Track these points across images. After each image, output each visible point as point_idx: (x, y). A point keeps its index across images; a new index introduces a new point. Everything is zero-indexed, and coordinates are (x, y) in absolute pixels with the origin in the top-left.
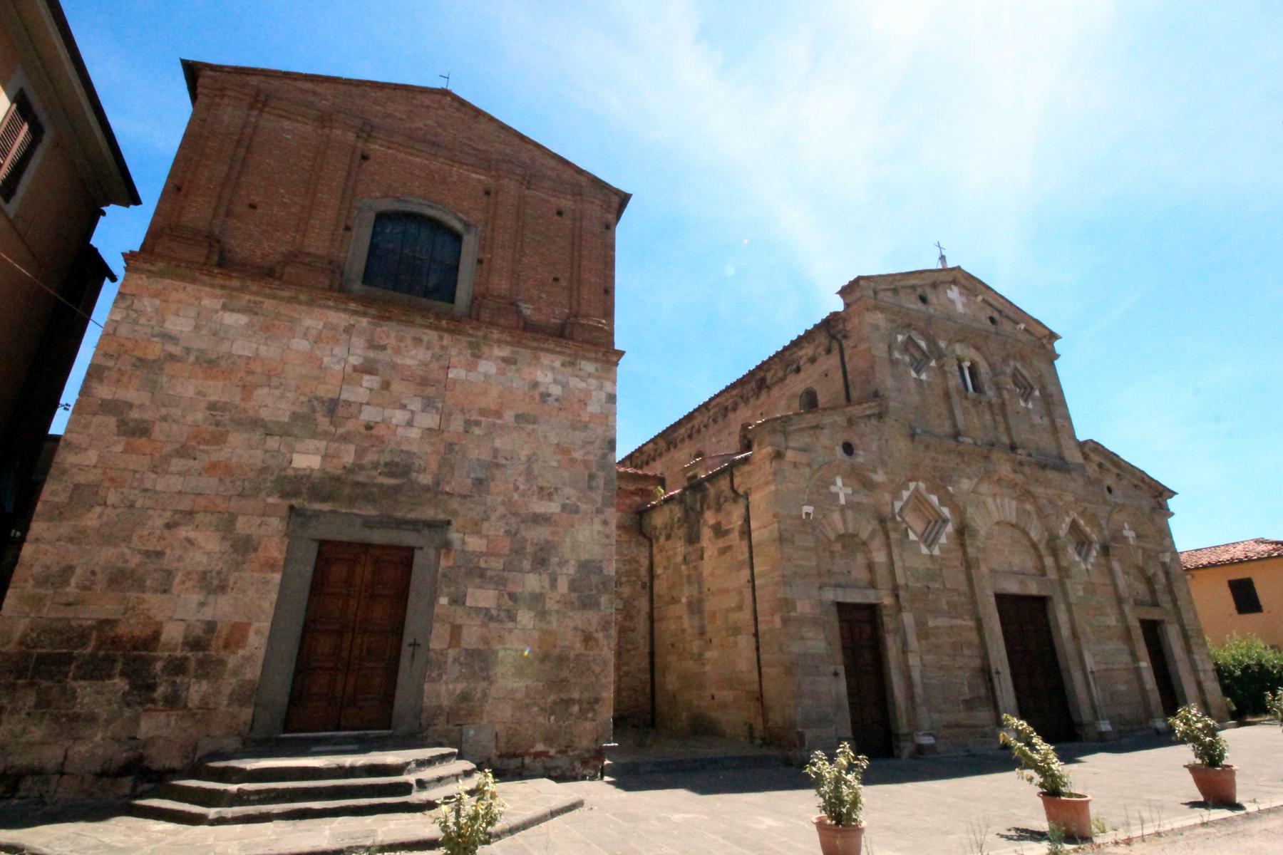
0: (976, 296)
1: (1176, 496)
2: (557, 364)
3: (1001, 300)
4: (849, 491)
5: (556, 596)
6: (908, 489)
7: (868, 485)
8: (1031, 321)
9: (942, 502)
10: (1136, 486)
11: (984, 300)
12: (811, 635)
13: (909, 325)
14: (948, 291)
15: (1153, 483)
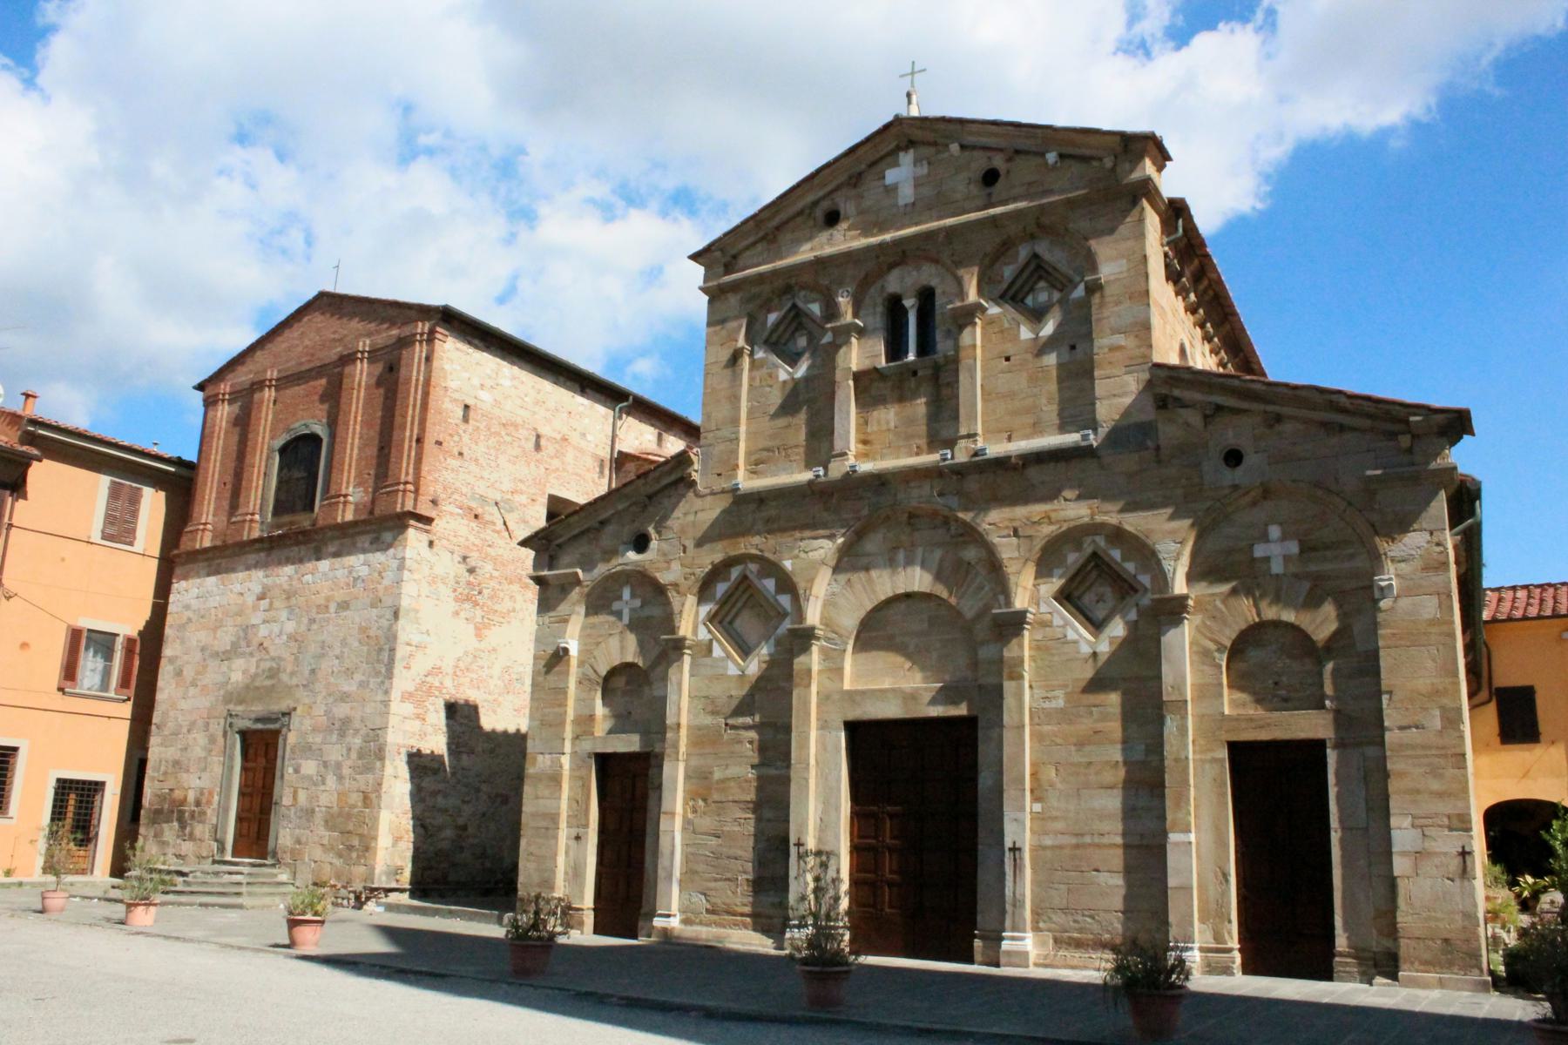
2: (367, 545)
3: (994, 127)
4: (637, 603)
5: (349, 763)
10: (1324, 425)
11: (963, 147)
13: (788, 290)
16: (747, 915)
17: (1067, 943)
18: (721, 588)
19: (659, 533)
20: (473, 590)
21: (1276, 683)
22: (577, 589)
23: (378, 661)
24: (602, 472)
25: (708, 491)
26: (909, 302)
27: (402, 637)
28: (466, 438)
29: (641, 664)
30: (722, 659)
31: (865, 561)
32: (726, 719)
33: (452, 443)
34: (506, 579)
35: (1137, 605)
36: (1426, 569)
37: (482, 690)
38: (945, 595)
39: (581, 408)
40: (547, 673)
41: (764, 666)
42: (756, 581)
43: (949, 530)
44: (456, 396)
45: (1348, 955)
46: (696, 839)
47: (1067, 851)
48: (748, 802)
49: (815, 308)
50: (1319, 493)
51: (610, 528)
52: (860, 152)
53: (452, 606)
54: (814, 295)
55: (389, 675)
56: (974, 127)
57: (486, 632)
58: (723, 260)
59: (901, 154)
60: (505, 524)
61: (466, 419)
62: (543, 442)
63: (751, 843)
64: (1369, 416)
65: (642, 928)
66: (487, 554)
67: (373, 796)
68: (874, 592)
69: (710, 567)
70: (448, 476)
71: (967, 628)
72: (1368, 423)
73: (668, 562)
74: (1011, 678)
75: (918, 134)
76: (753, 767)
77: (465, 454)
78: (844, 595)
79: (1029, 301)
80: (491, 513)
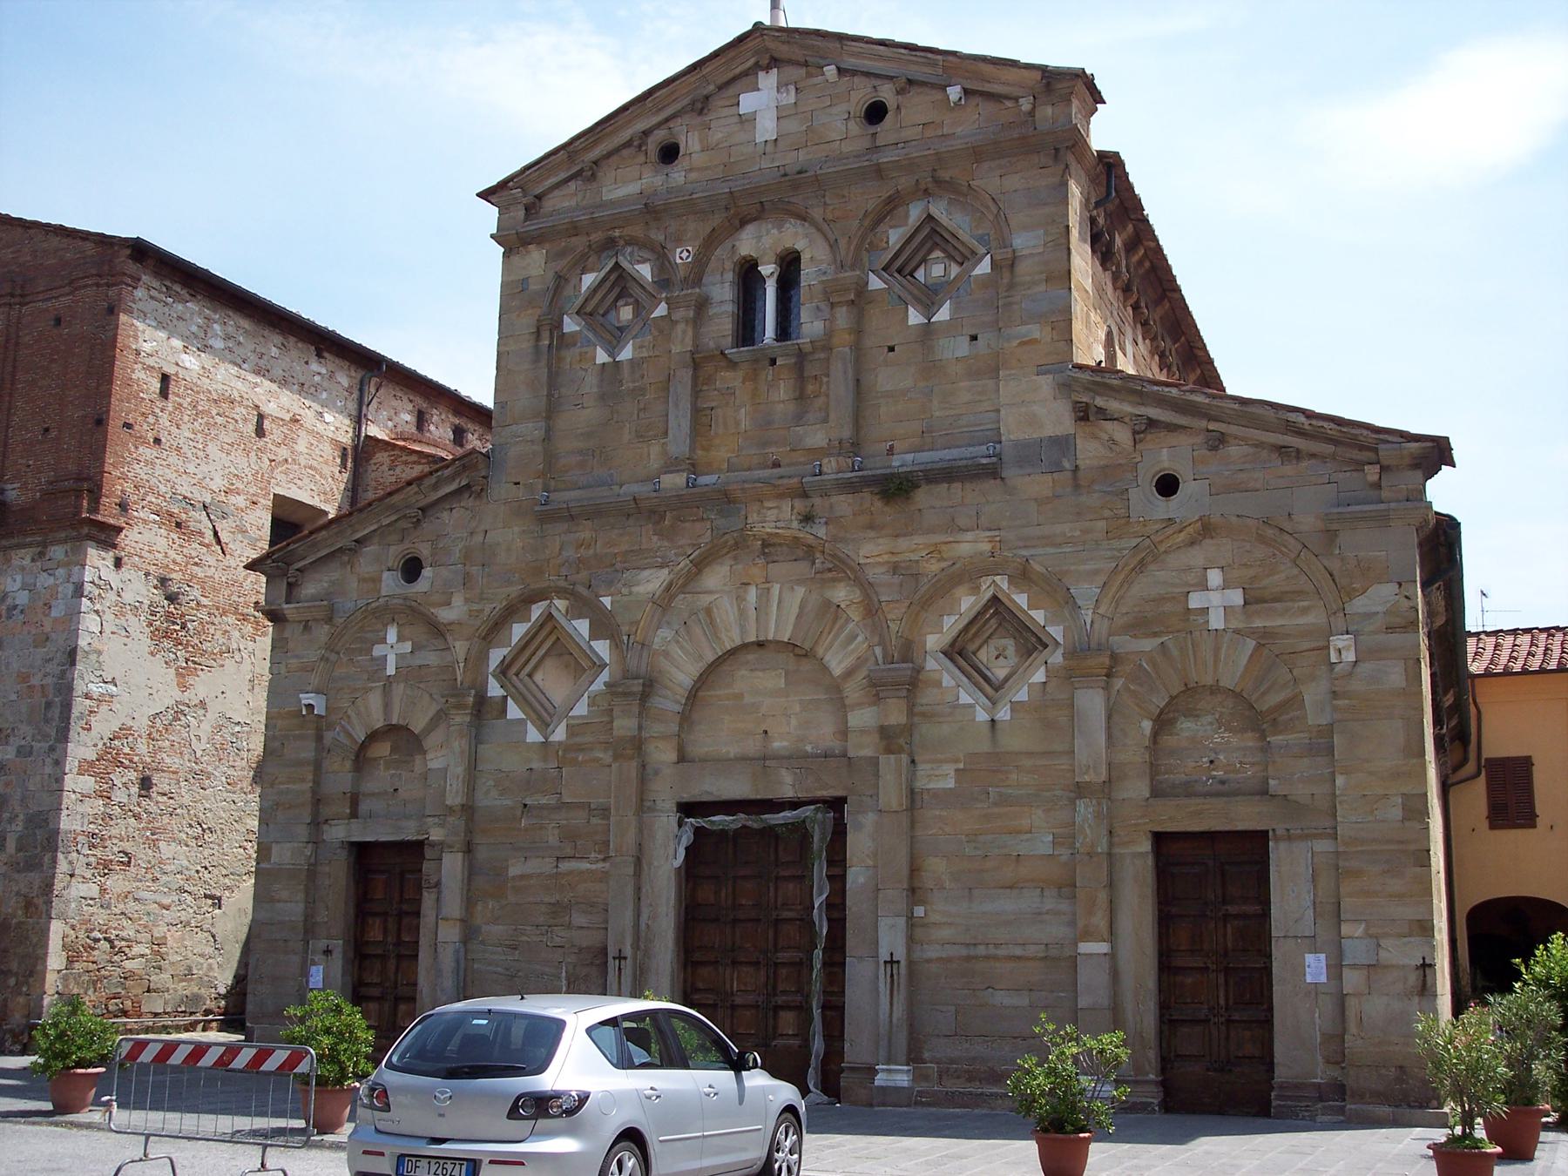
2: (27, 562)
7: (438, 631)
9: (594, 635)
10: (1281, 450)
12: (285, 894)
20: (174, 623)
21: (1212, 762)
23: (47, 721)
24: (344, 465)
26: (767, 269)
27: (79, 687)
28: (164, 420)
33: (145, 427)
34: (218, 610)
36: (1390, 629)
37: (186, 757)
39: (317, 378)
42: (563, 621)
43: (814, 563)
44: (150, 361)
49: (645, 271)
50: (1270, 532)
51: (371, 549)
52: (706, 70)
53: (146, 643)
54: (646, 254)
55: (63, 736)
57: (190, 680)
58: (525, 200)
59: (761, 74)
60: (216, 534)
61: (164, 393)
62: (267, 424)
66: (193, 576)
67: (40, 901)
70: (140, 470)
72: (1330, 448)
75: (783, 50)
77: (163, 440)
78: (678, 642)
79: (920, 275)
80: (199, 520)
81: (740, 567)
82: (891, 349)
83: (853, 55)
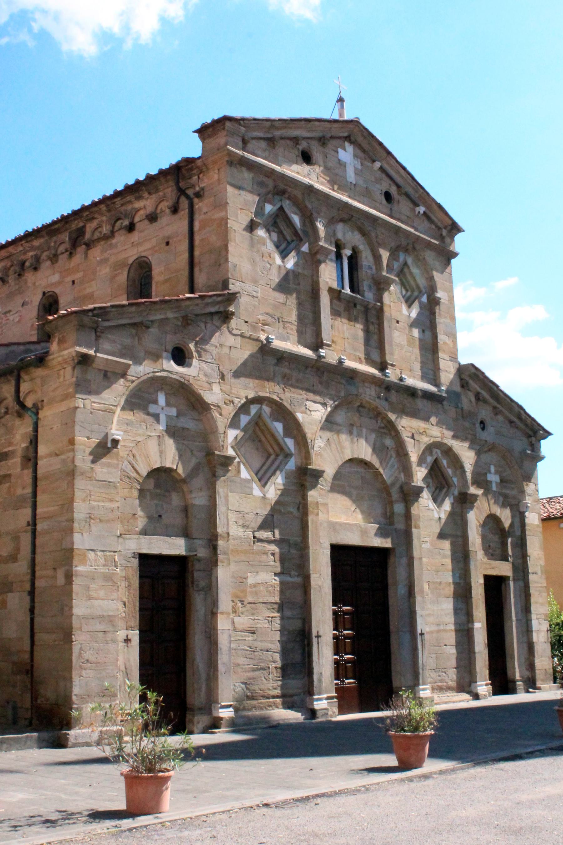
0: (374, 161)
1: (550, 437)
3: (402, 171)
4: (173, 412)
6: (247, 413)
8: (434, 204)
10: (511, 422)
11: (381, 169)
14: (340, 150)
15: (529, 421)
16: (277, 697)
17: (437, 690)
18: (244, 420)
19: (200, 356)
22: (122, 381)
25: (238, 332)
29: (180, 471)
30: (246, 481)
31: (335, 427)
32: (253, 532)
35: (453, 494)
38: (376, 462)
40: (93, 462)
41: (279, 492)
45: (521, 681)
46: (236, 636)
47: (434, 635)
48: (273, 603)
56: (392, 162)
63: (278, 636)
64: (526, 425)
65: (198, 723)
68: (343, 453)
69: (245, 400)
71: (385, 489)
73: (210, 384)
74: (416, 527)
76: (276, 574)
81: (349, 414)
82: (398, 322)
83: (391, 166)
